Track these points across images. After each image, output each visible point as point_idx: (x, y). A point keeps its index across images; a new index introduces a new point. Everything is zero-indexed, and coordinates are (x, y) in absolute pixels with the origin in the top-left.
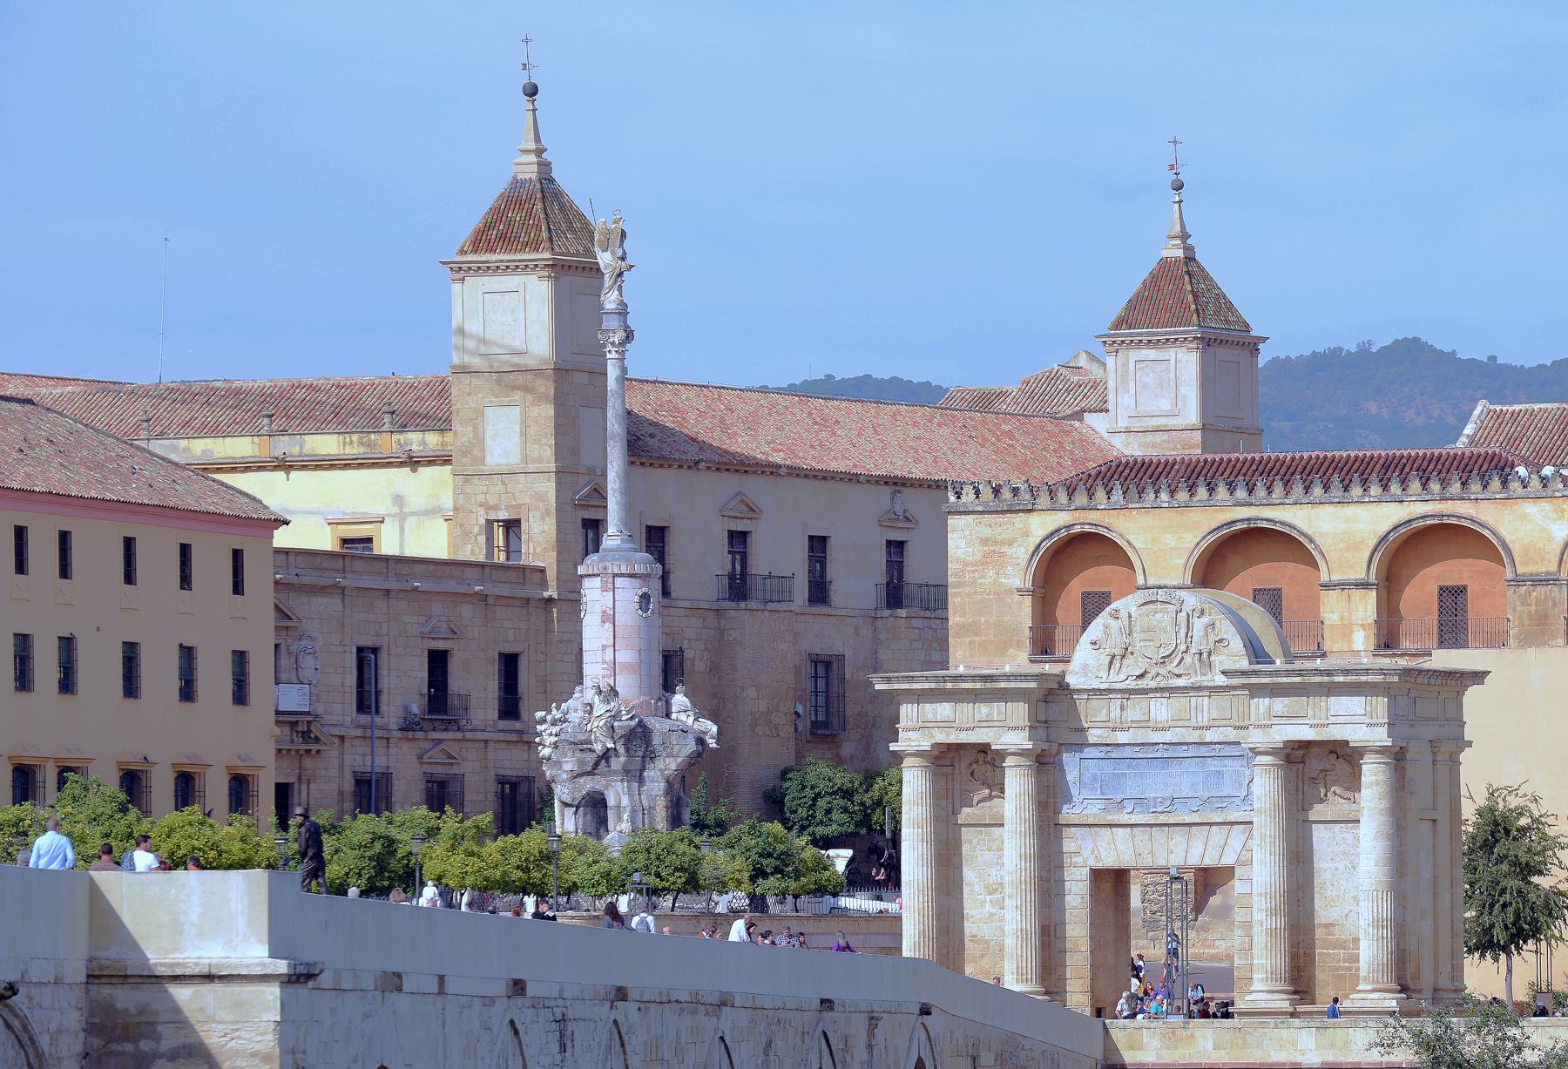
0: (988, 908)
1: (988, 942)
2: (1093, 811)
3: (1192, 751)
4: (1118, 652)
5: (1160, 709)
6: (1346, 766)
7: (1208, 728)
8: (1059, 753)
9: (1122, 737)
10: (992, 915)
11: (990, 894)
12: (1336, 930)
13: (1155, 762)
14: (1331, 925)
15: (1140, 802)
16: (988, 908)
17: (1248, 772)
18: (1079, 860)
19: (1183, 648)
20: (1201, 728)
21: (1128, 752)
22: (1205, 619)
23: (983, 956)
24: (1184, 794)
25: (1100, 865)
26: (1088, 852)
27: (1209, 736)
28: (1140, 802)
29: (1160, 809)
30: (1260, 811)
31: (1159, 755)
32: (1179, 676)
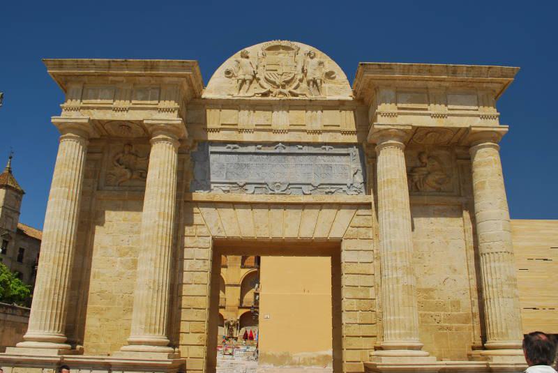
0: (118, 267)
2: (217, 194)
3: (306, 149)
4: (249, 77)
5: (281, 119)
6: (436, 163)
7: (319, 132)
8: (193, 147)
9: (246, 137)
11: (121, 256)
13: (273, 157)
14: (432, 290)
15: (260, 185)
16: (118, 267)
17: (353, 166)
18: (204, 230)
19: (300, 76)
20: (315, 132)
21: (252, 149)
22: (316, 60)
24: (299, 181)
25: (222, 235)
26: (212, 224)
27: (320, 138)
28: (260, 185)
29: (276, 192)
30: (389, 182)
31: (277, 151)
32: (297, 95)
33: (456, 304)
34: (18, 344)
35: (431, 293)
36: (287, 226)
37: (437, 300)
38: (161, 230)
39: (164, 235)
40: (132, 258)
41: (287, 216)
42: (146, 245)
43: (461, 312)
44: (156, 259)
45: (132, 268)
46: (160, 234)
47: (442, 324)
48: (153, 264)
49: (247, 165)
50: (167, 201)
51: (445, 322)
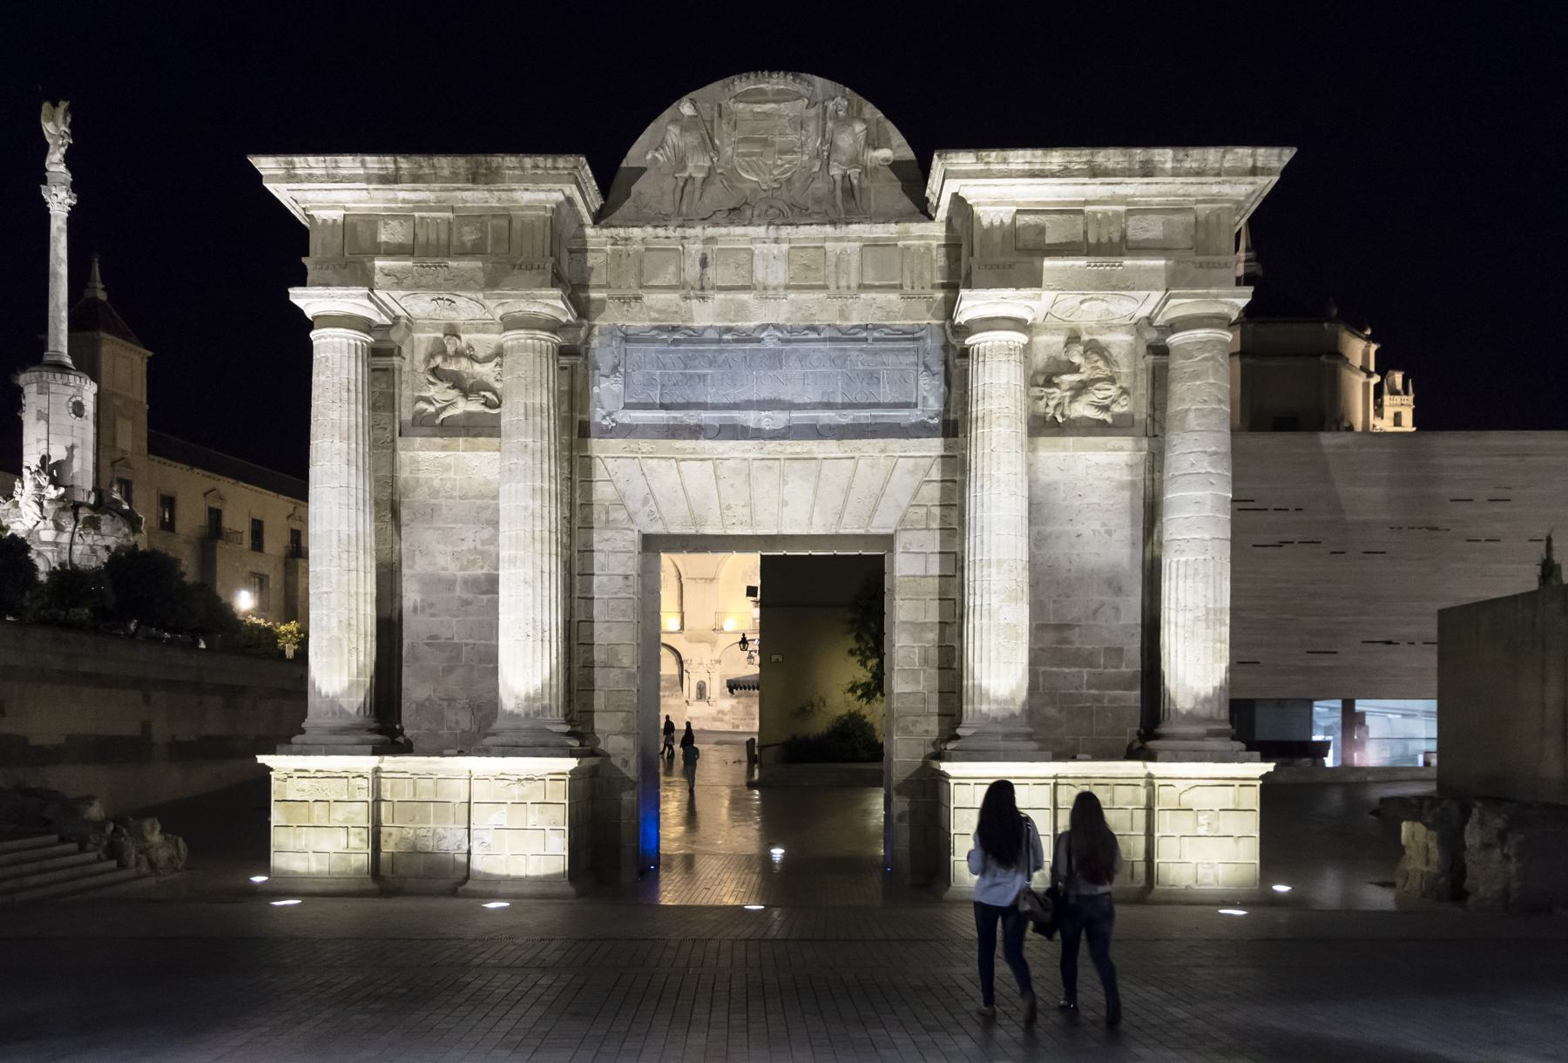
1: (458, 647)
10: (467, 603)
12: (1075, 635)
14: (1069, 627)
23: (448, 671)
33: (1117, 653)
34: (294, 740)
35: (1066, 634)
36: (784, 503)
37: (1077, 645)
38: (538, 523)
39: (546, 534)
40: (485, 571)
41: (785, 482)
42: (513, 552)
43: (1123, 669)
44: (534, 579)
45: (486, 592)
46: (538, 534)
47: (1085, 691)
48: (530, 591)
49: (702, 377)
50: (546, 466)
51: (1089, 688)
